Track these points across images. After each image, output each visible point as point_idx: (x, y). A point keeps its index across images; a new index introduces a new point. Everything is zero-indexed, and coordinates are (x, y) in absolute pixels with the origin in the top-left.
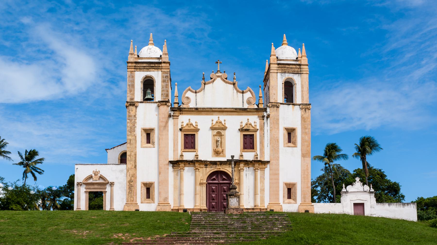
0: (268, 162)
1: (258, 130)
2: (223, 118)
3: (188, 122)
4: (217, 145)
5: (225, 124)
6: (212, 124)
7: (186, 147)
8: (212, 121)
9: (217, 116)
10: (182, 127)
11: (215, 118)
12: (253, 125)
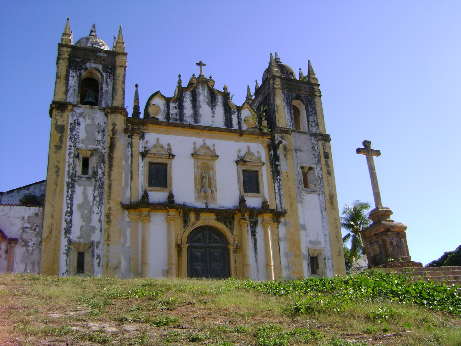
0: (282, 214)
1: (264, 163)
2: (209, 142)
3: (155, 142)
4: (203, 183)
5: (214, 150)
6: (195, 148)
7: (151, 184)
8: (195, 143)
9: (203, 139)
10: (147, 149)
11: (199, 141)
12: (256, 154)
